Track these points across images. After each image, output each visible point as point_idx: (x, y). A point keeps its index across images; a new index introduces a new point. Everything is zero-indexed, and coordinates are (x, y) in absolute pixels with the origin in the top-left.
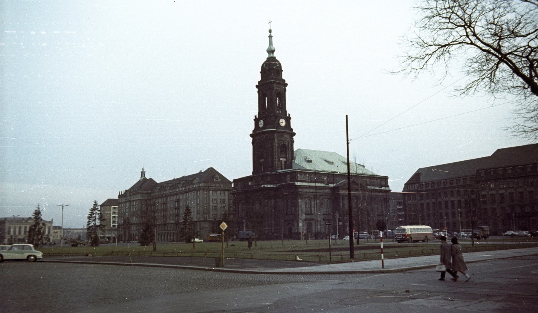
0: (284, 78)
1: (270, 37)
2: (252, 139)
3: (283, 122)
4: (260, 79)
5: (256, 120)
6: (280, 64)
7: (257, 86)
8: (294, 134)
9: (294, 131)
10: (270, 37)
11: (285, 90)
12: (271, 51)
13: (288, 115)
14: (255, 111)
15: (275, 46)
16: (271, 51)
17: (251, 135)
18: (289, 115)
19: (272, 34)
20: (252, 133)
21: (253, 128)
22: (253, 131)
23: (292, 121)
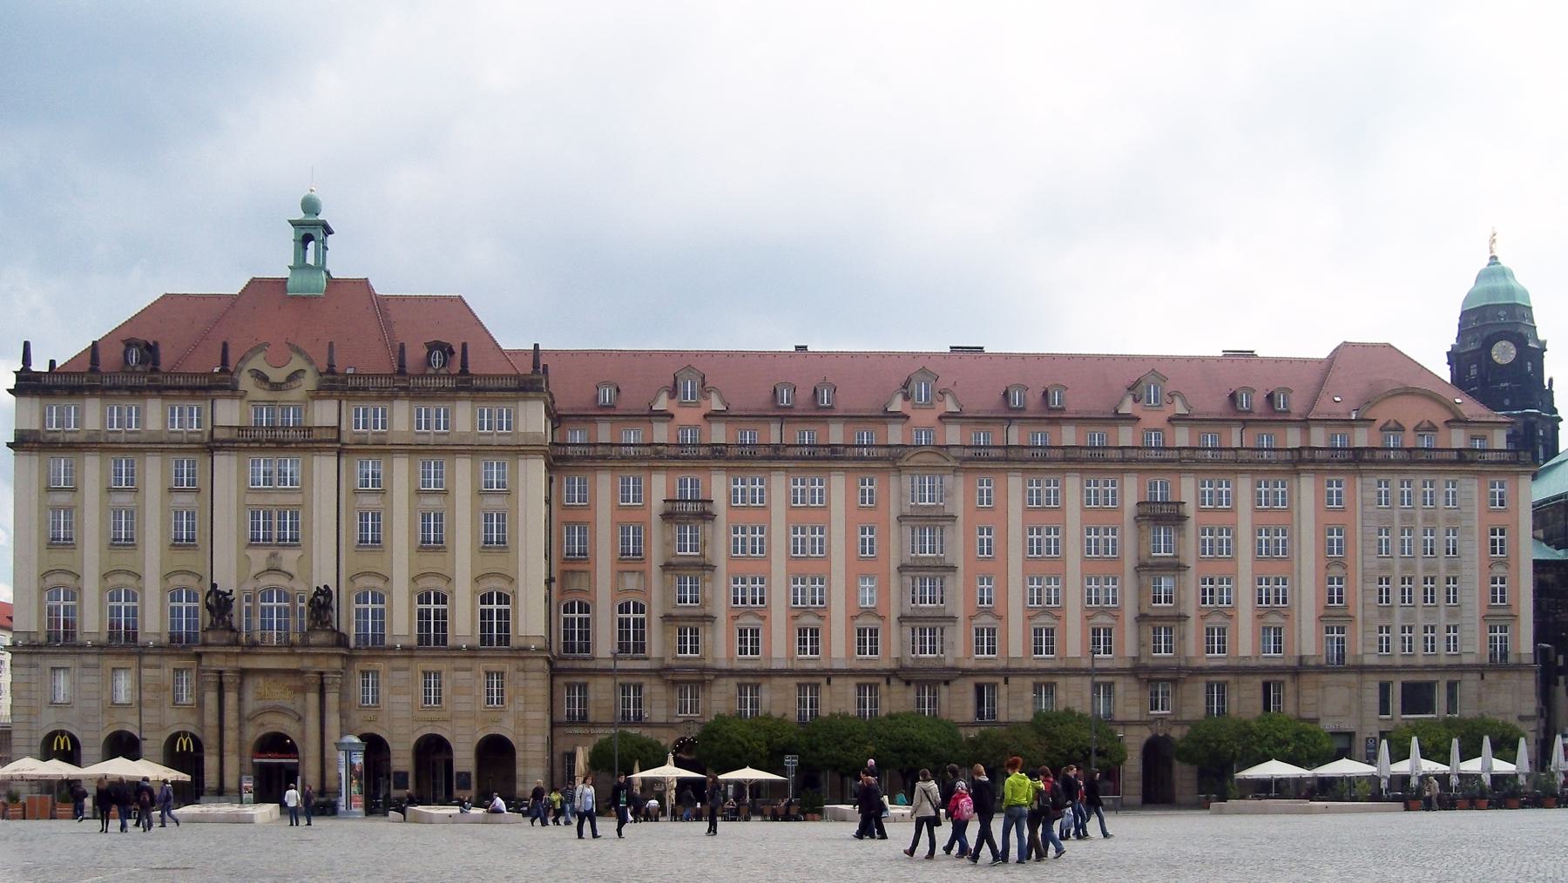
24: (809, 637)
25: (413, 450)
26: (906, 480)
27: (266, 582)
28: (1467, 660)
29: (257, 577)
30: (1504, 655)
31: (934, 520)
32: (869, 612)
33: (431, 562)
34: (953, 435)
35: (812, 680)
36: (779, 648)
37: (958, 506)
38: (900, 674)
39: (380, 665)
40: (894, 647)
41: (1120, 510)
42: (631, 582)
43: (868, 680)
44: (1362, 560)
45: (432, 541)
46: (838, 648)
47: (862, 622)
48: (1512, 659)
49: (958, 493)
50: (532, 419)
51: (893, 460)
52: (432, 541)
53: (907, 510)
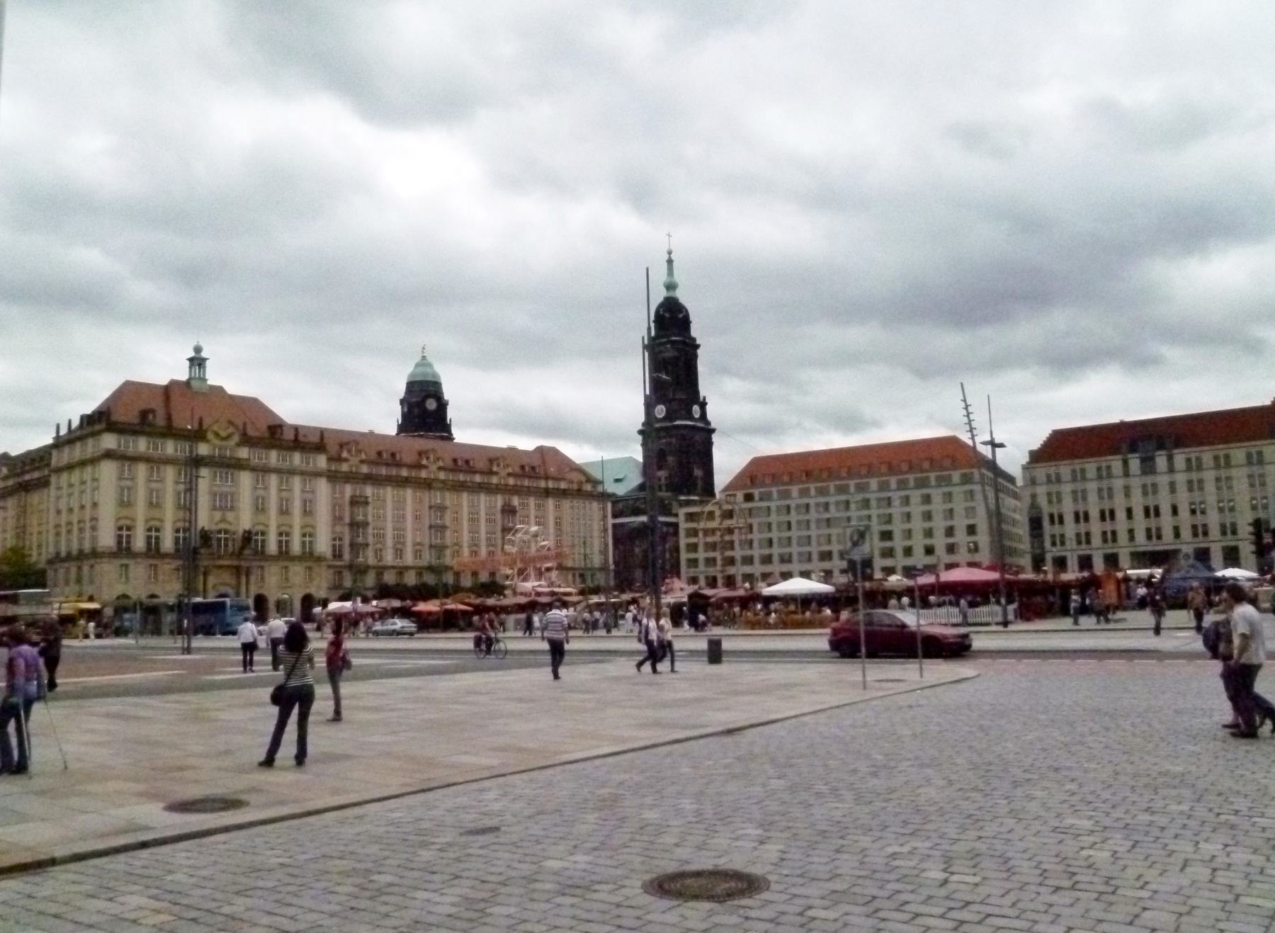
1: (670, 262)
3: (696, 408)
5: (649, 406)
6: (687, 311)
8: (713, 431)
9: (713, 425)
10: (670, 262)
11: (696, 356)
12: (671, 286)
13: (701, 399)
15: (678, 277)
16: (671, 286)
17: (641, 432)
18: (704, 398)
19: (673, 256)
21: (642, 418)
23: (709, 408)
24: (399, 552)
25: (278, 471)
26: (432, 492)
27: (223, 526)
29: (217, 524)
31: (441, 509)
32: (419, 544)
34: (442, 475)
35: (401, 571)
36: (389, 558)
37: (448, 503)
38: (430, 569)
39: (266, 564)
40: (427, 558)
41: (495, 507)
42: (338, 529)
43: (420, 571)
44: (566, 527)
45: (284, 511)
46: (409, 559)
47: (417, 547)
49: (449, 498)
50: (321, 462)
51: (428, 485)
52: (284, 511)
53: (433, 504)
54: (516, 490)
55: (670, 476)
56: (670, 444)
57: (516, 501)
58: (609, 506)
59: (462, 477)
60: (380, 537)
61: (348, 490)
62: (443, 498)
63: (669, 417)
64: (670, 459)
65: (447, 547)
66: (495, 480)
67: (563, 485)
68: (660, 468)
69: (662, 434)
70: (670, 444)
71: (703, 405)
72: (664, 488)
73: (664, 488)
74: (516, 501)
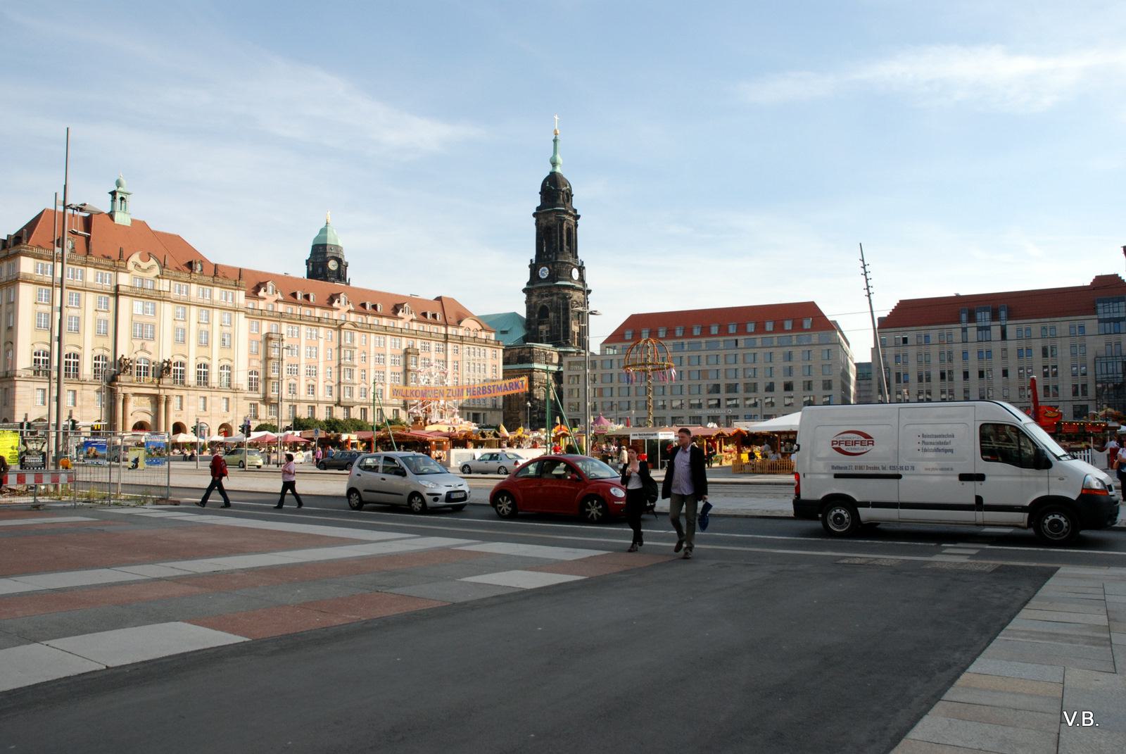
0: (575, 206)
1: (555, 141)
2: (525, 296)
4: (539, 204)
5: (534, 268)
7: (535, 215)
10: (555, 141)
11: (576, 226)
12: (554, 164)
14: (532, 254)
17: (525, 291)
20: (525, 286)
21: (527, 278)
22: (528, 284)
28: (488, 407)
30: (496, 406)
33: (204, 351)
48: (498, 407)
54: (415, 335)
55: (551, 331)
56: (551, 301)
57: (418, 344)
58: (501, 351)
59: (371, 320)
60: (294, 371)
61: (266, 327)
62: (352, 340)
63: (553, 277)
64: (551, 315)
65: (356, 384)
66: (400, 324)
67: (461, 332)
68: (541, 323)
69: (545, 292)
70: (551, 301)
71: (581, 269)
72: (544, 340)
73: (544, 340)
74: (418, 344)
